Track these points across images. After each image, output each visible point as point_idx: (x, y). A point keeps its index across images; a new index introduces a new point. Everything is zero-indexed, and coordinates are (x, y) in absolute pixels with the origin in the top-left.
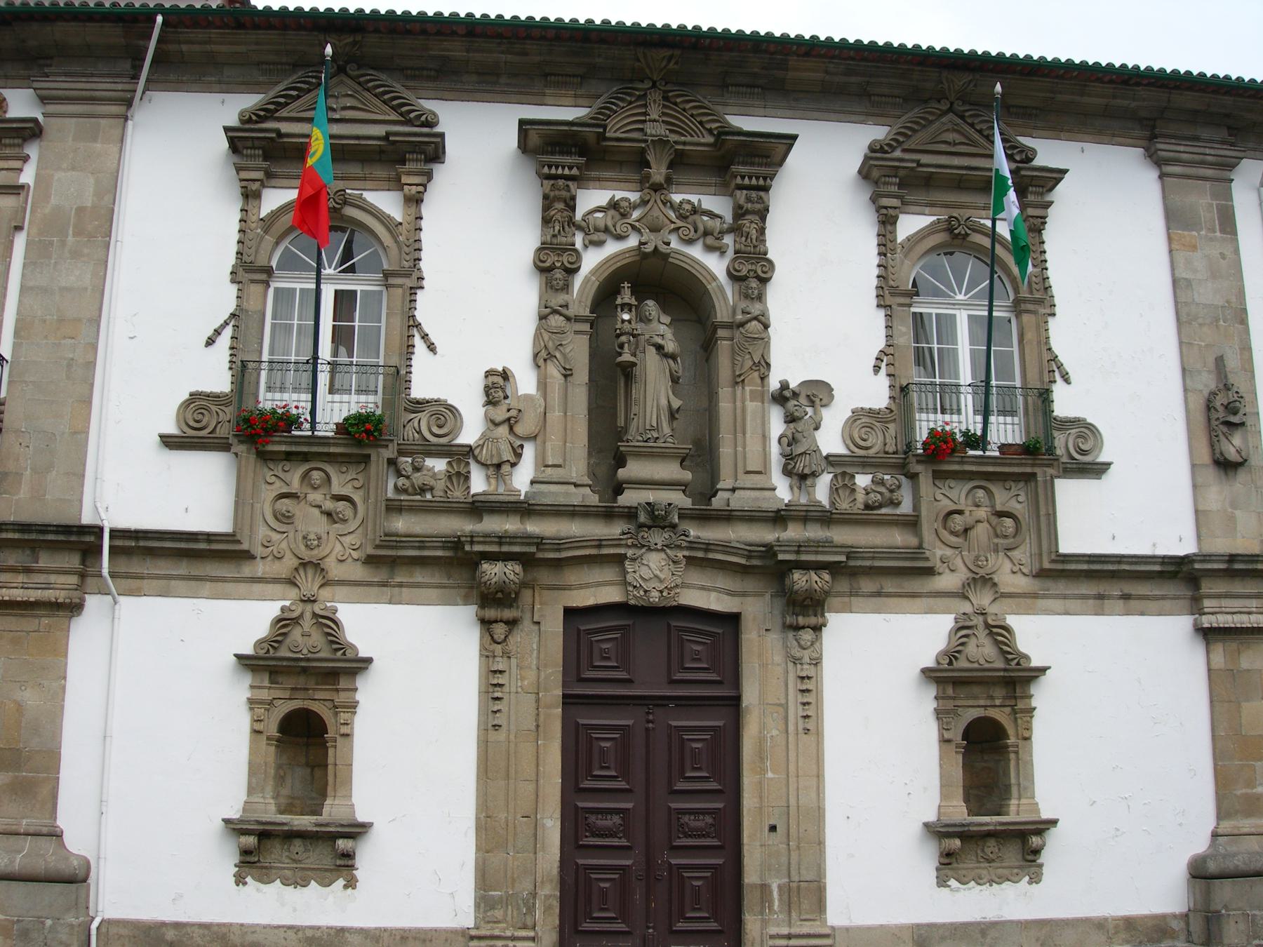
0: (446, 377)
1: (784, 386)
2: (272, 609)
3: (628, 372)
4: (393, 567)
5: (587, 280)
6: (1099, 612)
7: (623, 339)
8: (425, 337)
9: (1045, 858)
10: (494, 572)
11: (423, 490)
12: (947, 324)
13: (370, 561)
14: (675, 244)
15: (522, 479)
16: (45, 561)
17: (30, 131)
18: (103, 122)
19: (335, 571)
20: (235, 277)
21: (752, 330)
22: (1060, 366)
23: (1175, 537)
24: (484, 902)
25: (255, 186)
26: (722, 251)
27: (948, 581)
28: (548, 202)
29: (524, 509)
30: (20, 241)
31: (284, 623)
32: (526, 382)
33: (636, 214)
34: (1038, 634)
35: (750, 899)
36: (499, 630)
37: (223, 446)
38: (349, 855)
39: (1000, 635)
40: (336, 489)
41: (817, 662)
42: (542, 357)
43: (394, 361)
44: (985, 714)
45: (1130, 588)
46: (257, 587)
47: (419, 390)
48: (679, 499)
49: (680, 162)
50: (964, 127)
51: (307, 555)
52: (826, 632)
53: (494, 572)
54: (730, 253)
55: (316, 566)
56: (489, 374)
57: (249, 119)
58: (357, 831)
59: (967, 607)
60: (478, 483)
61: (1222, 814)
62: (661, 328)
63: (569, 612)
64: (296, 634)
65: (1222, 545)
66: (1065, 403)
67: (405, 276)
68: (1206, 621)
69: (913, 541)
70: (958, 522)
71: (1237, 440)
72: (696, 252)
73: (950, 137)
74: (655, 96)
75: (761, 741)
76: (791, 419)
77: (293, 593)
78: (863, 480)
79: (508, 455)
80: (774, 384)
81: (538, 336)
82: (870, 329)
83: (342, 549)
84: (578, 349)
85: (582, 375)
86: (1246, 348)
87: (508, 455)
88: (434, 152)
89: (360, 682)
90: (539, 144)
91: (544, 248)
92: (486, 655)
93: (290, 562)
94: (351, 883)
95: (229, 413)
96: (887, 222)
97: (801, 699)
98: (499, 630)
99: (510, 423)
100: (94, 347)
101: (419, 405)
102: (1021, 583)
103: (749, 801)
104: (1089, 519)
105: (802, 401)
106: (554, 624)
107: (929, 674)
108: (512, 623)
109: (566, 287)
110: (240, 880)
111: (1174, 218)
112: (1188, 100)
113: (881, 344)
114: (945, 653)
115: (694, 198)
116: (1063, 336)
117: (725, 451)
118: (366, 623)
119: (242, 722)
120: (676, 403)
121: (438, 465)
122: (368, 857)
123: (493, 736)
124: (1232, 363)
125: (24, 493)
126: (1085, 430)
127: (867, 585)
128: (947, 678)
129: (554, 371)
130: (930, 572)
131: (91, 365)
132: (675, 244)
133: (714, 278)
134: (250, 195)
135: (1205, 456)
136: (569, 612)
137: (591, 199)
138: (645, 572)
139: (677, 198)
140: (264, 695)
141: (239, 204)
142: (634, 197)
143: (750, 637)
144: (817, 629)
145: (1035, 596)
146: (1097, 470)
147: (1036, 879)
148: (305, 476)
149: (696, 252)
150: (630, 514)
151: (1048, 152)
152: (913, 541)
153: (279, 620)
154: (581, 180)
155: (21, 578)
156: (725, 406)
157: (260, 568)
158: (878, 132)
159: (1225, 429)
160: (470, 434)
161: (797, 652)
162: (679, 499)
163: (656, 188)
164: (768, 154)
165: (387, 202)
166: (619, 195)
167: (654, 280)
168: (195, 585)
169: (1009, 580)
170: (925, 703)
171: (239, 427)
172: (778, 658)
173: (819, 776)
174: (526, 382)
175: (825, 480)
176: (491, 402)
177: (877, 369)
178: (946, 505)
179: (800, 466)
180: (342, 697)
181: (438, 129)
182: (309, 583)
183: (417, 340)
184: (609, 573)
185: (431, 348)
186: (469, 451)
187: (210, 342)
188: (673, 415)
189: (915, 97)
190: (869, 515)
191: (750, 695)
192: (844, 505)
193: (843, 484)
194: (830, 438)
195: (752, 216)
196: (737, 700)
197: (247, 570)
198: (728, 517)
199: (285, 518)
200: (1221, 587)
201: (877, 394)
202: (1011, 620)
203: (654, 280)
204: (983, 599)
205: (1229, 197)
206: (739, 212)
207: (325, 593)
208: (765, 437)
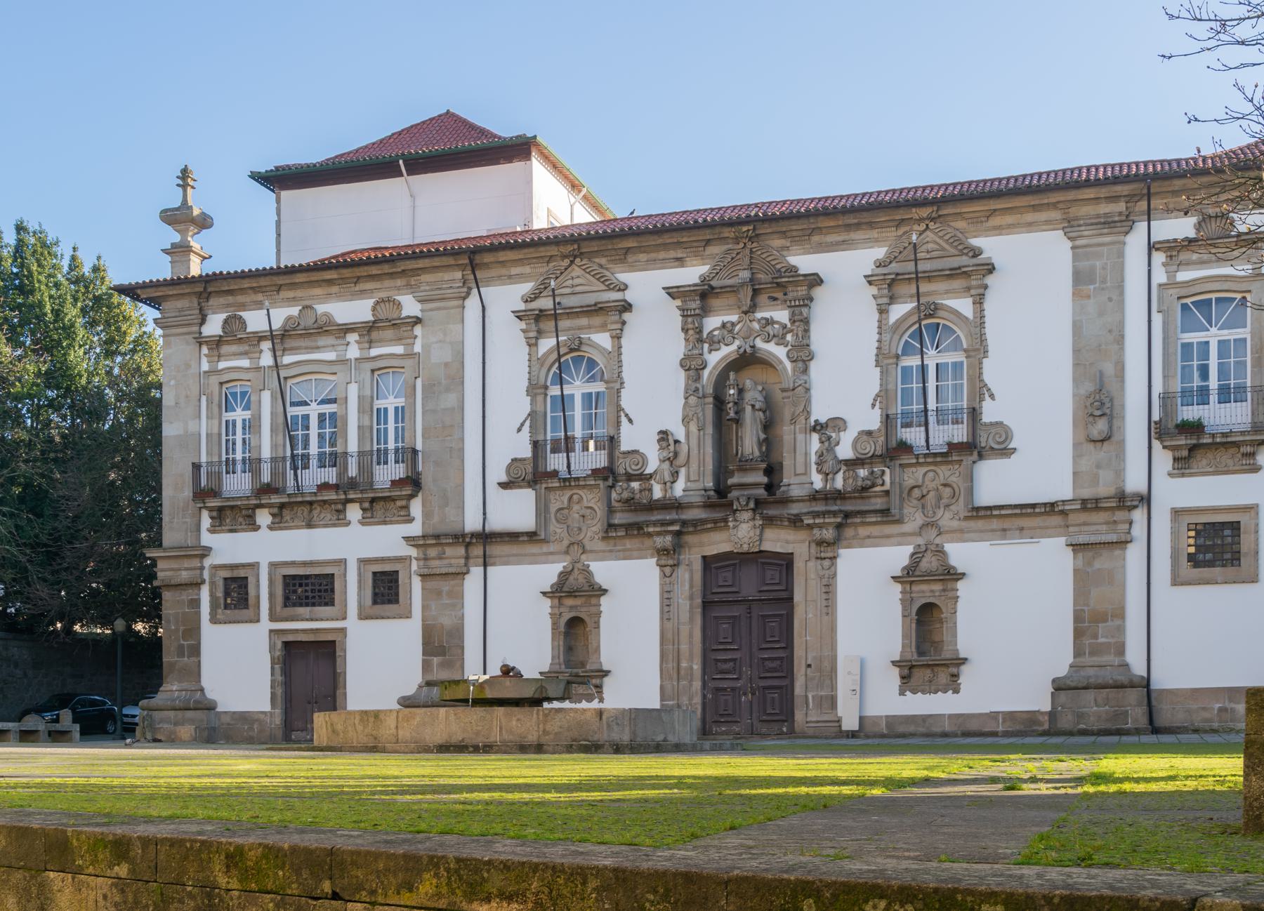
0: (638, 438)
1: (816, 421)
2: (557, 568)
5: (711, 373)
6: (1004, 538)
7: (731, 405)
8: (627, 415)
9: (962, 680)
12: (923, 368)
14: (759, 343)
15: (679, 489)
16: (449, 551)
17: (418, 321)
18: (452, 311)
19: (588, 547)
20: (528, 393)
21: (801, 392)
22: (989, 390)
23: (1061, 488)
25: (533, 341)
27: (908, 527)
30: (419, 382)
31: (564, 576)
32: (680, 433)
34: (959, 553)
36: (668, 570)
39: (940, 552)
40: (585, 503)
41: (835, 575)
42: (686, 420)
46: (551, 557)
47: (624, 447)
48: (761, 492)
52: (839, 561)
55: (580, 544)
56: (661, 432)
59: (920, 541)
60: (658, 493)
63: (704, 558)
64: (571, 578)
65: (1086, 493)
66: (990, 412)
67: (616, 383)
70: (917, 493)
71: (1101, 425)
77: (568, 558)
82: (871, 381)
85: (710, 430)
87: (667, 477)
88: (627, 307)
89: (603, 600)
91: (687, 357)
92: (662, 585)
93: (566, 543)
95: (530, 469)
97: (824, 596)
98: (668, 570)
100: (462, 440)
102: (955, 524)
106: (698, 566)
109: (698, 378)
113: (877, 389)
114: (904, 568)
115: (767, 315)
118: (603, 570)
120: (762, 436)
121: (635, 485)
123: (669, 625)
125: (436, 519)
129: (693, 428)
131: (462, 450)
133: (781, 362)
134: (532, 344)
136: (704, 558)
137: (712, 323)
138: (740, 534)
140: (556, 611)
142: (734, 318)
143: (798, 565)
145: (961, 531)
146: (1006, 452)
148: (570, 498)
153: (561, 573)
154: (705, 311)
155: (437, 563)
157: (552, 548)
159: (1091, 419)
161: (821, 573)
165: (603, 340)
166: (727, 318)
168: (519, 559)
172: (813, 576)
177: (873, 406)
178: (910, 482)
179: (825, 468)
180: (593, 609)
183: (624, 419)
185: (630, 421)
186: (651, 476)
187: (519, 430)
188: (760, 444)
191: (798, 597)
194: (845, 450)
196: (791, 599)
197: (545, 548)
198: (786, 501)
200: (1083, 517)
201: (873, 421)
202: (950, 548)
204: (932, 533)
207: (583, 557)
208: (806, 454)
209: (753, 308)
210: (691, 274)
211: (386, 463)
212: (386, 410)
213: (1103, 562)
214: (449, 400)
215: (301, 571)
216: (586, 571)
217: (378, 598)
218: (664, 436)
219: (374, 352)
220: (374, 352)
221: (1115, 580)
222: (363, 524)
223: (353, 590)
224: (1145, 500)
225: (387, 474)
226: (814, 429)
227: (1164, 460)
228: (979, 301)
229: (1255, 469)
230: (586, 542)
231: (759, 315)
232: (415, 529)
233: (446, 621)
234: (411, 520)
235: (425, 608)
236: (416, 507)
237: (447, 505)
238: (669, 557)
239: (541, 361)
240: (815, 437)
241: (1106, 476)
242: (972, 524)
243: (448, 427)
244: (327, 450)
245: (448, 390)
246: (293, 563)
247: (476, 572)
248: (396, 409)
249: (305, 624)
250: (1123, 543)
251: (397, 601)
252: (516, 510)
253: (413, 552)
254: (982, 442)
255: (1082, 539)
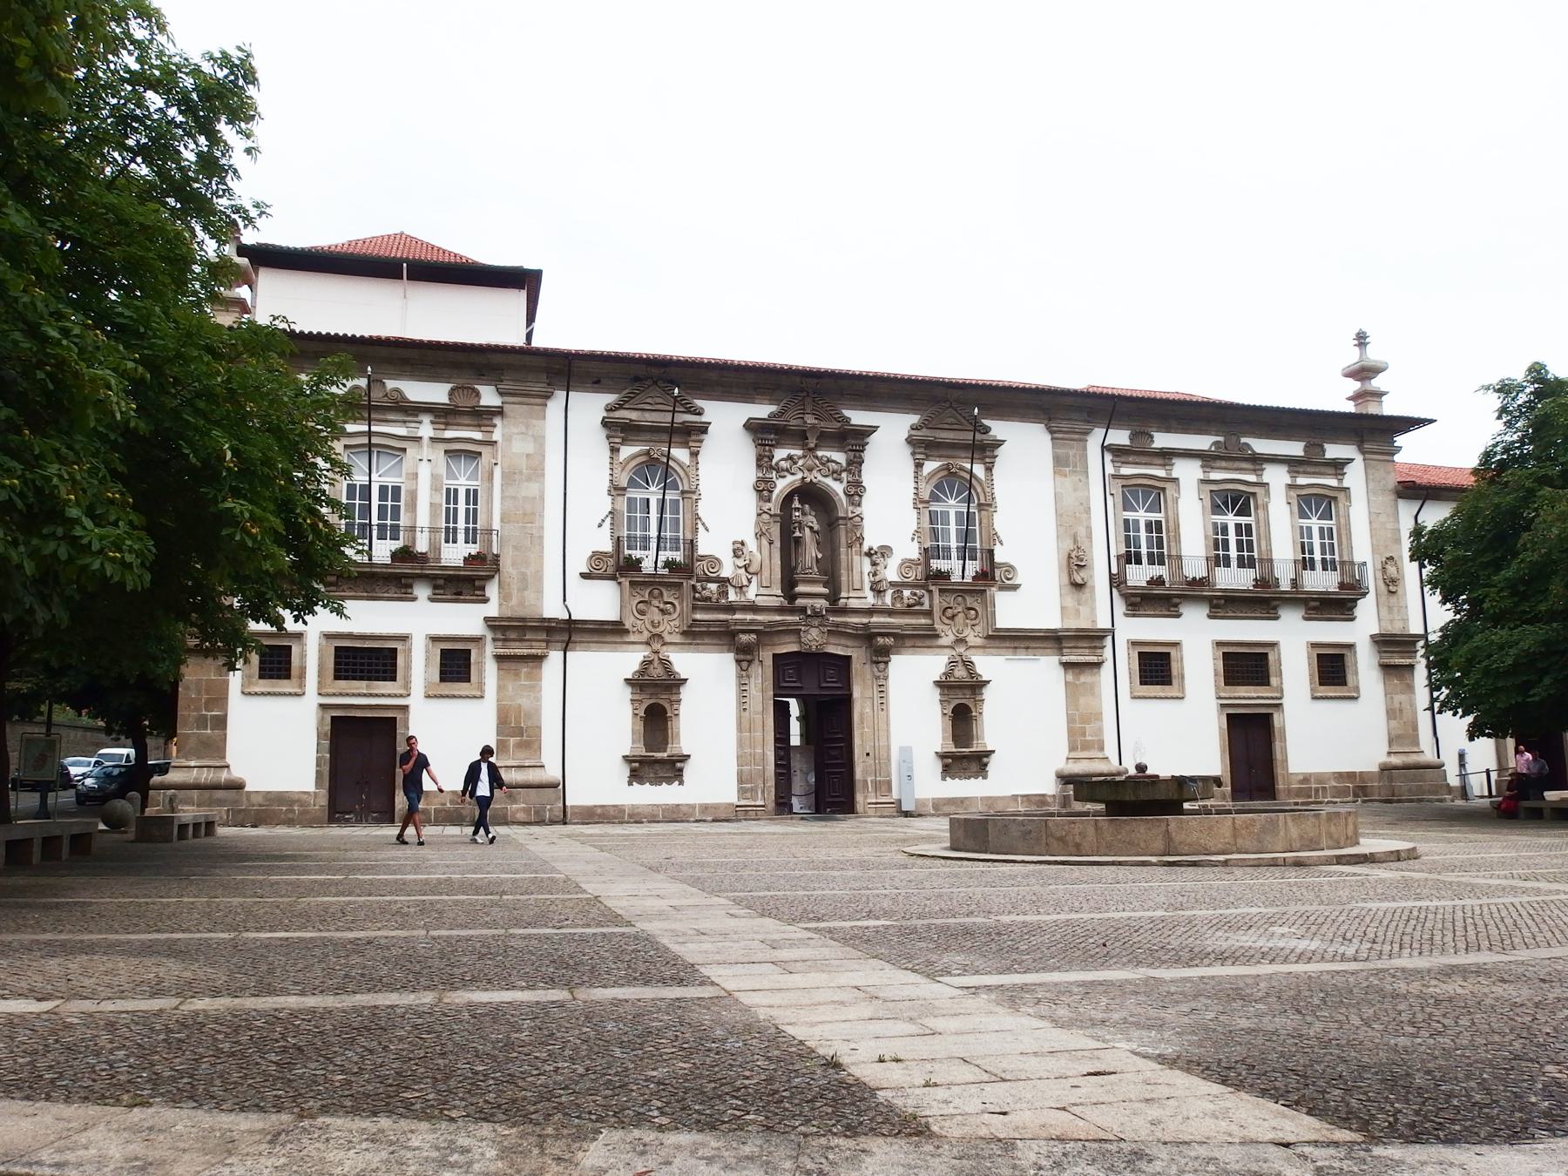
3: (798, 541)
4: (695, 635)
10: (744, 638)
11: (709, 599)
13: (684, 633)
14: (820, 478)
15: (752, 593)
19: (668, 638)
21: (855, 524)
23: (1050, 620)
24: (742, 792)
26: (840, 480)
27: (944, 641)
28: (759, 459)
29: (753, 608)
30: (497, 472)
31: (647, 663)
33: (801, 462)
34: (987, 665)
35: (859, 786)
36: (745, 665)
37: (613, 578)
38: (681, 770)
39: (969, 665)
41: (886, 678)
42: (759, 535)
43: (689, 537)
44: (962, 700)
45: (1027, 644)
46: (631, 647)
48: (821, 603)
49: (826, 439)
50: (956, 418)
51: (655, 631)
53: (744, 638)
54: (845, 483)
55: (660, 636)
57: (609, 409)
58: (685, 758)
60: (732, 596)
61: (1072, 748)
62: (811, 520)
65: (1073, 624)
66: (999, 558)
68: (1064, 659)
69: (929, 621)
71: (1083, 574)
72: (829, 481)
73: (950, 420)
74: (809, 400)
75: (862, 714)
76: (874, 564)
78: (907, 593)
79: (745, 582)
80: (865, 548)
81: (757, 523)
83: (670, 627)
84: (776, 530)
85: (777, 544)
86: (1089, 529)
87: (745, 582)
90: (753, 427)
91: (759, 480)
92: (740, 677)
93: (646, 635)
94: (681, 783)
95: (611, 562)
96: (919, 466)
98: (745, 665)
99: (746, 567)
101: (703, 557)
102: (979, 641)
103: (857, 741)
104: (1010, 612)
105: (878, 555)
106: (769, 662)
107: (938, 684)
108: (750, 662)
109: (769, 500)
110: (630, 784)
111: (1059, 462)
112: (1069, 401)
116: (1001, 522)
117: (844, 579)
118: (684, 662)
119: (627, 710)
121: (713, 587)
122: (689, 771)
124: (1082, 531)
125: (514, 602)
126: (1010, 568)
127: (909, 643)
128: (945, 686)
129: (765, 542)
130: (938, 636)
131: (541, 537)
132: (820, 478)
134: (614, 450)
135: (1066, 580)
137: (780, 454)
139: (820, 453)
141: (608, 453)
143: (856, 666)
144: (886, 663)
146: (1015, 588)
147: (985, 777)
149: (829, 481)
150: (803, 610)
151: (998, 428)
152: (929, 621)
154: (778, 445)
156: (843, 557)
157: (632, 638)
158: (914, 419)
160: (727, 572)
162: (821, 603)
163: (810, 450)
164: (865, 433)
165: (681, 454)
166: (793, 452)
167: (810, 494)
169: (973, 639)
170: (936, 694)
171: (618, 567)
173: (888, 731)
174: (752, 545)
175: (890, 592)
176: (736, 556)
180: (674, 698)
181: (704, 419)
182: (657, 646)
184: (793, 638)
189: (935, 400)
190: (909, 611)
192: (898, 605)
193: (898, 596)
194: (891, 573)
195: (856, 463)
198: (845, 611)
199: (642, 613)
201: (913, 552)
202: (974, 659)
203: (810, 494)
204: (961, 649)
205: (1085, 449)
206: (850, 463)
209: (817, 447)
210: (762, 411)
211: (455, 541)
212: (456, 491)
213: (1086, 678)
214: (530, 489)
215: (358, 644)
216: (666, 664)
217: (446, 676)
218: (738, 550)
219: (449, 434)
220: (449, 434)
221: (1092, 690)
222: (432, 600)
223: (419, 666)
224: (1112, 631)
225: (454, 555)
226: (869, 554)
227: (1120, 607)
228: (989, 469)
229: (1178, 616)
230: (665, 635)
231: (820, 453)
232: (492, 609)
233: (524, 702)
234: (486, 601)
235: (500, 688)
236: (492, 590)
237: (525, 588)
238: (745, 656)
239: (624, 465)
240: (867, 561)
241: (1084, 610)
242: (992, 643)
243: (527, 516)
244: (389, 522)
245: (529, 479)
246: (350, 636)
247: (555, 656)
248: (468, 491)
249: (363, 696)
250: (1098, 665)
251: (468, 680)
252: (600, 602)
253: (489, 636)
254: (990, 576)
255: (1073, 659)
